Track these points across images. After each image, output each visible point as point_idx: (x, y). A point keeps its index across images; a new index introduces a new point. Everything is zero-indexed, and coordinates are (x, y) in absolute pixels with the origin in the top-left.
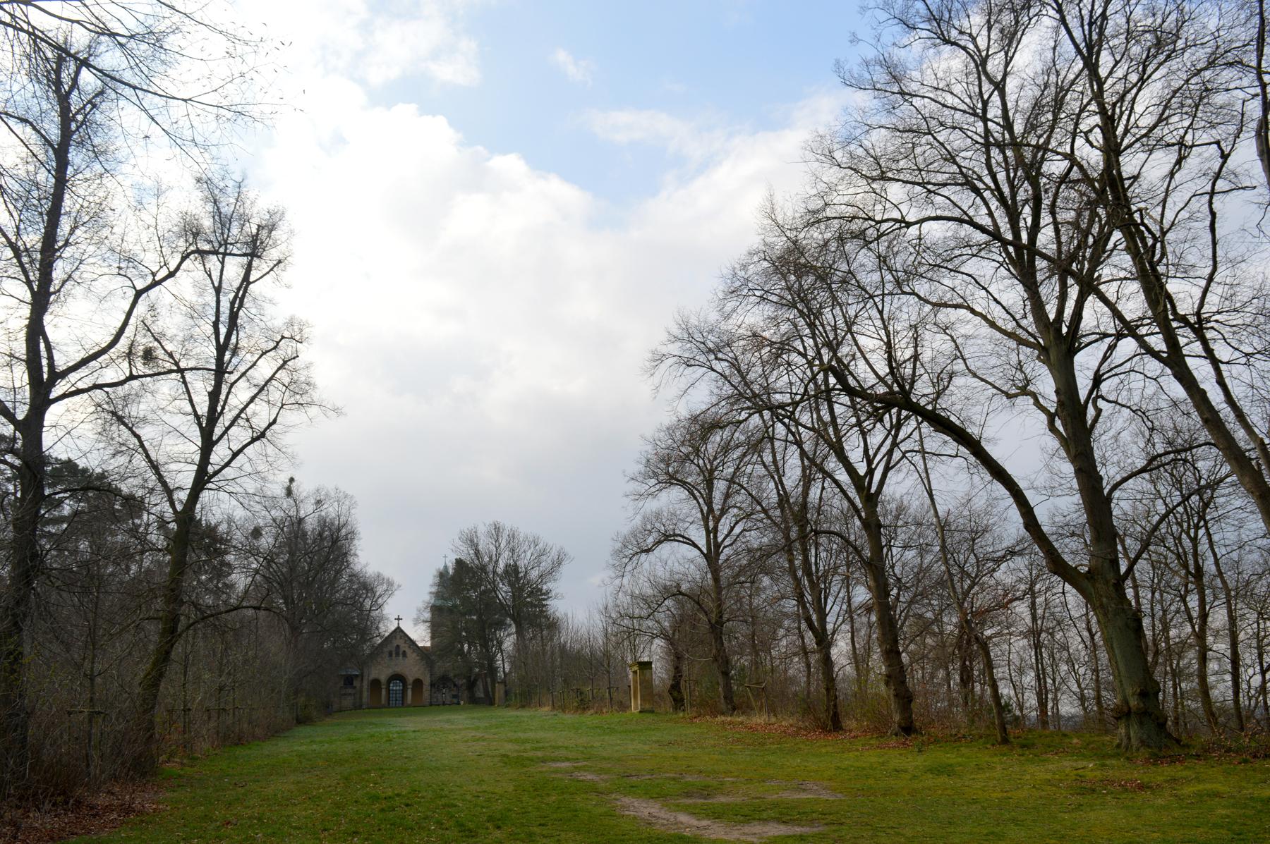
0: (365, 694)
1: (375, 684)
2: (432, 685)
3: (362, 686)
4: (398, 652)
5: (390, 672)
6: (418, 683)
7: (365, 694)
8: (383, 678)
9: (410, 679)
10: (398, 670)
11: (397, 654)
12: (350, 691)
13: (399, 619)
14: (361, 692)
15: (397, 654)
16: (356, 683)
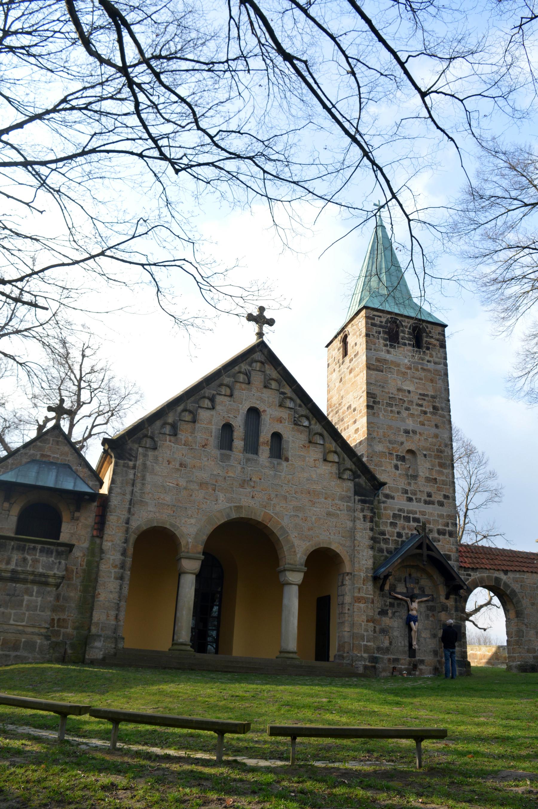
0: (109, 588)
1: (155, 546)
2: (379, 580)
3: (96, 553)
4: (249, 437)
5: (220, 507)
6: (323, 563)
7: (109, 589)
8: (192, 530)
9: (297, 549)
10: (253, 503)
11: (252, 446)
12: (42, 563)
13: (260, 319)
14: (91, 580)
15: (252, 446)
16: (75, 530)
